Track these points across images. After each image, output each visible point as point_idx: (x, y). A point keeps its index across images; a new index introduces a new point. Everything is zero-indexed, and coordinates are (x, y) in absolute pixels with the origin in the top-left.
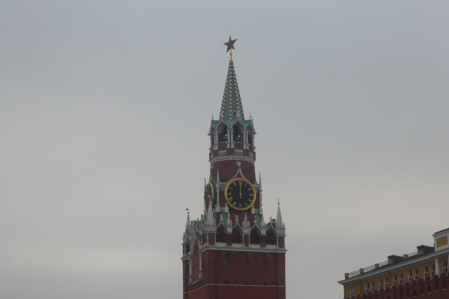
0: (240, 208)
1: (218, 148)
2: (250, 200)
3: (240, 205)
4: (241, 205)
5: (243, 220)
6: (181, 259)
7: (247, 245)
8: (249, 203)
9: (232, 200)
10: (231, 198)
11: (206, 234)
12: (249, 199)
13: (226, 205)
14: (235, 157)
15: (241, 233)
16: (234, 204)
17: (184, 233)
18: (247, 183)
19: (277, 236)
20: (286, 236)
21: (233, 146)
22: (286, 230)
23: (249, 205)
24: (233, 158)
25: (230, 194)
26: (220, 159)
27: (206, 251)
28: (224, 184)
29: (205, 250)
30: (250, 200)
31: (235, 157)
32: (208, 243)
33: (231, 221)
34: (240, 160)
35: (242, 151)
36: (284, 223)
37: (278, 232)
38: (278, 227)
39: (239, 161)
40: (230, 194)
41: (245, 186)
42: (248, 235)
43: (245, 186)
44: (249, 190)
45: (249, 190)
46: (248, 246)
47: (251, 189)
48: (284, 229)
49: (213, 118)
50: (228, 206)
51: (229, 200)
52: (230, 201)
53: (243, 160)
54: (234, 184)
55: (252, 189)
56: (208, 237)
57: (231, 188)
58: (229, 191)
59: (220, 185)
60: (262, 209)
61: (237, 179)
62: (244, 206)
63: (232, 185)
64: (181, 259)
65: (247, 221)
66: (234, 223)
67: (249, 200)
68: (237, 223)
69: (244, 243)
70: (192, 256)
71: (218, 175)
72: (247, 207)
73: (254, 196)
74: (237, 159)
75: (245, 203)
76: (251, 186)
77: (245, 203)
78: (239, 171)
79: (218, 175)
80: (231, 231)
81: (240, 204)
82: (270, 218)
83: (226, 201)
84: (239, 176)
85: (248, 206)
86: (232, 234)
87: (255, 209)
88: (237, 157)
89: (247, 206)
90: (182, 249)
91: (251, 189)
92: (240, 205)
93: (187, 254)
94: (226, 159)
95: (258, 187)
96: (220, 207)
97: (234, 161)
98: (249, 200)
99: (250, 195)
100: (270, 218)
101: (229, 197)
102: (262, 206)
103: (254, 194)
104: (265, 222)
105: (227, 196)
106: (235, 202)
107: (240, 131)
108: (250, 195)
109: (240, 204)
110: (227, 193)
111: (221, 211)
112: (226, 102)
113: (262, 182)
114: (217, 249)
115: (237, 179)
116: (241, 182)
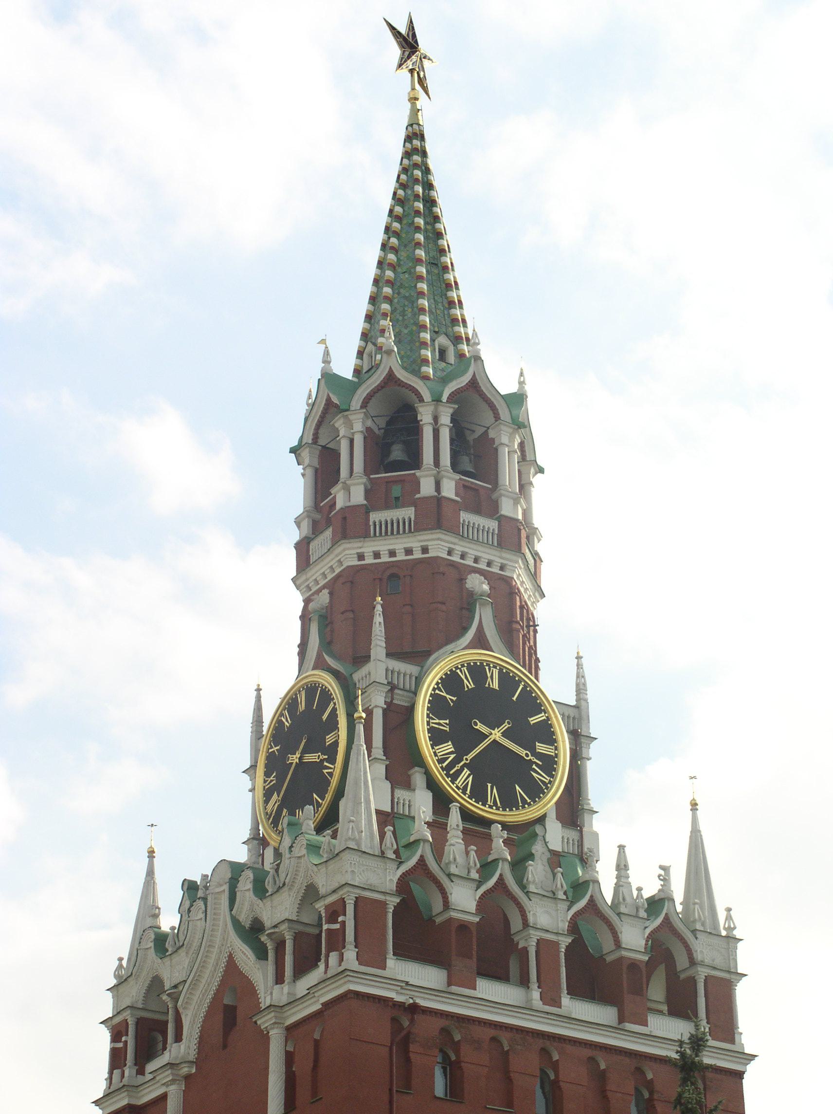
0: (491, 807)
1: (366, 498)
3: (493, 793)
4: (495, 790)
5: (531, 856)
6: (97, 1103)
7: (551, 998)
8: (536, 791)
9: (453, 756)
11: (343, 901)
13: (418, 779)
15: (516, 924)
16: (460, 781)
17: (121, 959)
18: (525, 687)
19: (702, 973)
20: (744, 979)
21: (449, 490)
22: (740, 945)
25: (444, 724)
26: (377, 555)
27: (327, 1005)
28: (408, 672)
29: (324, 999)
31: (459, 549)
32: (350, 954)
33: (467, 853)
34: (482, 566)
35: (493, 525)
36: (729, 910)
37: (703, 950)
38: (703, 924)
40: (444, 724)
41: (514, 698)
42: (557, 944)
43: (514, 698)
44: (533, 720)
45: (533, 720)
46: (558, 1004)
48: (732, 940)
49: (326, 360)
50: (432, 785)
51: (436, 755)
52: (440, 761)
53: (495, 570)
54: (463, 677)
55: (548, 718)
56: (349, 918)
57: (448, 696)
58: (437, 706)
59: (387, 670)
60: (596, 835)
61: (477, 655)
62: (509, 802)
63: (451, 681)
64: (97, 1103)
65: (548, 869)
66: (487, 867)
67: (534, 774)
68: (503, 869)
69: (534, 985)
70: (185, 1070)
71: (381, 619)
74: (469, 562)
75: (517, 788)
76: (540, 705)
78: (481, 619)
79: (378, 619)
80: (472, 906)
81: (489, 785)
82: (661, 867)
83: (420, 762)
84: (481, 642)
85: (529, 804)
86: (478, 923)
87: (562, 826)
88: (473, 551)
90: (108, 1049)
92: (493, 793)
93: (141, 1072)
94: (409, 551)
95: (574, 718)
96: (388, 785)
97: (453, 564)
98: (534, 774)
100: (661, 867)
101: (437, 738)
102: (595, 816)
104: (639, 889)
105: (427, 735)
107: (480, 431)
109: (489, 785)
111: (392, 808)
112: (396, 300)
113: (592, 695)
114: (398, 993)
115: (477, 655)
116: (496, 673)
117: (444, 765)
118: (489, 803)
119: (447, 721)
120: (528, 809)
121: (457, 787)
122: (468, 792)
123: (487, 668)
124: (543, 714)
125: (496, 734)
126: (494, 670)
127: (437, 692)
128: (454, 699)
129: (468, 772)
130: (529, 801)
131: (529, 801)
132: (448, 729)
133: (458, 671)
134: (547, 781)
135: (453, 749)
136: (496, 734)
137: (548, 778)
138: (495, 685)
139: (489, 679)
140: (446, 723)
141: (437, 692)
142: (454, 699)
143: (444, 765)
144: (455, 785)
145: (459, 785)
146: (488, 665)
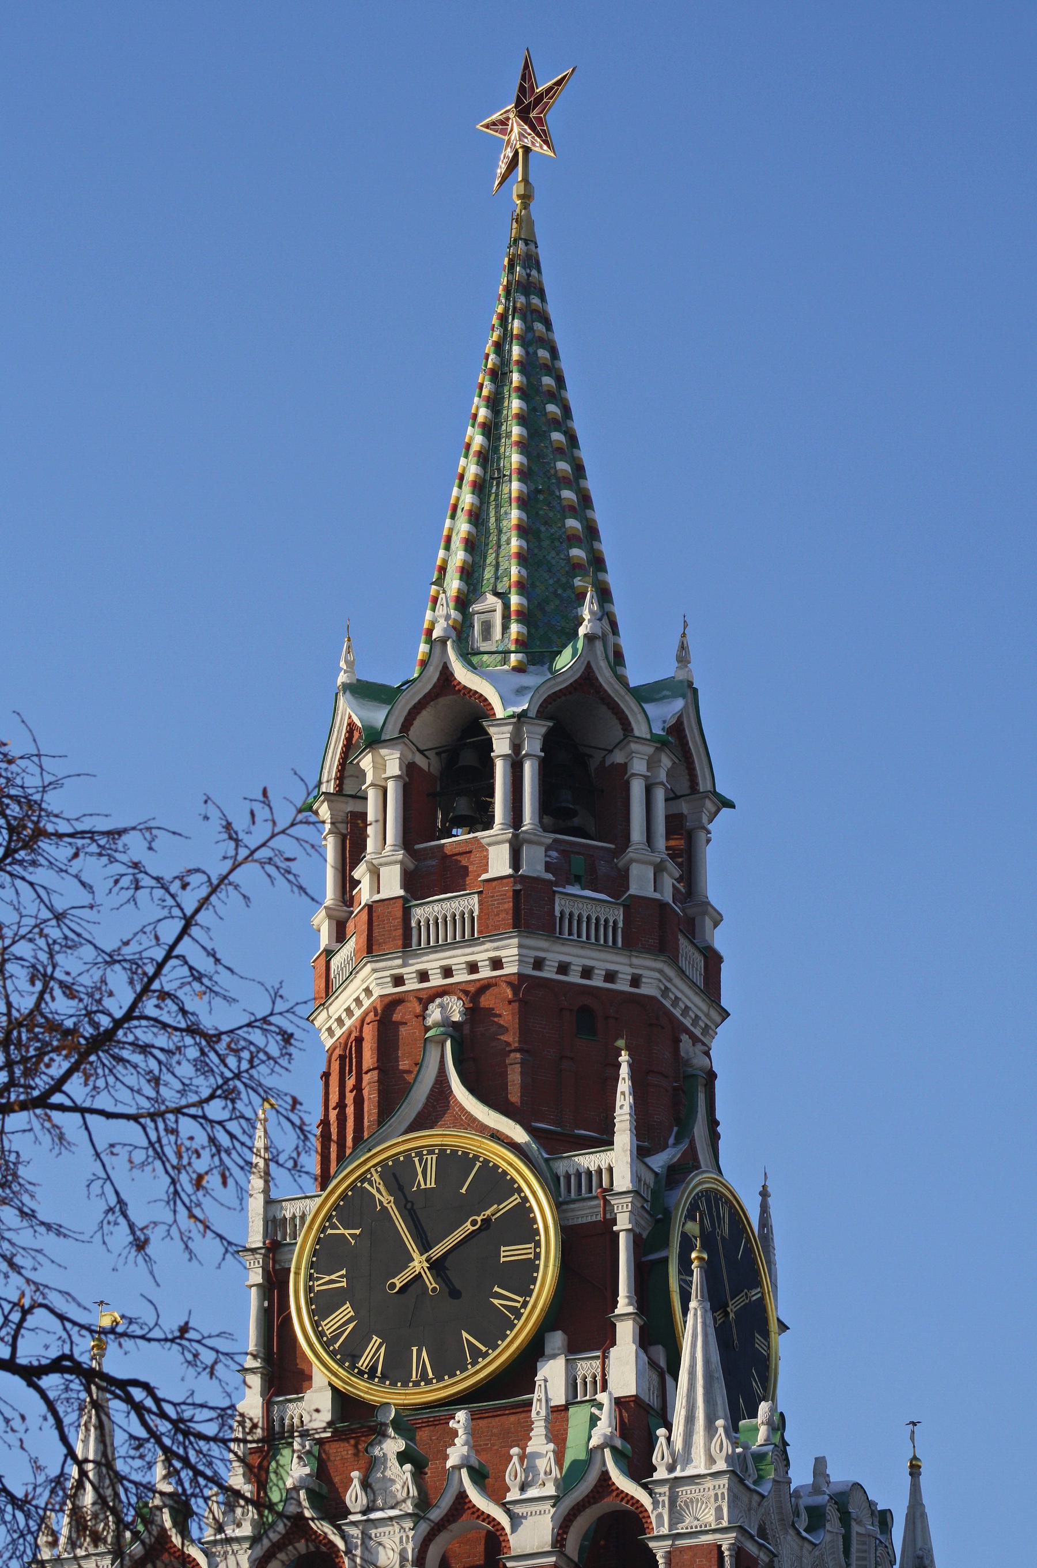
2: (502, 1299)
3: (420, 1358)
4: (424, 1354)
10: (346, 1311)
12: (496, 1289)
14: (409, 971)
23: (495, 1347)
24: (398, 981)
30: (502, 1299)
39: (442, 992)
40: (338, 1280)
41: (463, 1191)
43: (463, 1191)
47: (514, 1200)
67: (496, 1302)
72: (474, 1363)
73: (537, 1256)
77: (465, 1335)
81: (415, 1349)
85: (485, 1355)
89: (477, 1354)
91: (514, 1200)
98: (496, 1302)
99: (508, 1253)
103: (538, 1244)
106: (376, 1340)
108: (508, 1253)
109: (415, 1349)
110: (311, 1277)
116: (432, 1160)
117: (337, 1346)
118: (414, 1378)
119: (344, 1272)
120: (482, 1362)
121: (361, 1373)
122: (379, 1374)
123: (416, 1160)
124: (516, 1196)
125: (419, 1263)
126: (429, 1157)
127: (329, 1231)
128: (358, 1232)
129: (379, 1340)
130: (484, 1349)
131: (484, 1349)
132: (344, 1284)
133: (366, 1185)
134: (518, 1305)
135: (352, 1313)
136: (419, 1263)
137: (521, 1299)
138: (431, 1184)
139: (420, 1177)
140: (341, 1276)
141: (329, 1231)
142: (358, 1232)
143: (337, 1346)
144: (356, 1370)
145: (363, 1368)
146: (420, 1155)
